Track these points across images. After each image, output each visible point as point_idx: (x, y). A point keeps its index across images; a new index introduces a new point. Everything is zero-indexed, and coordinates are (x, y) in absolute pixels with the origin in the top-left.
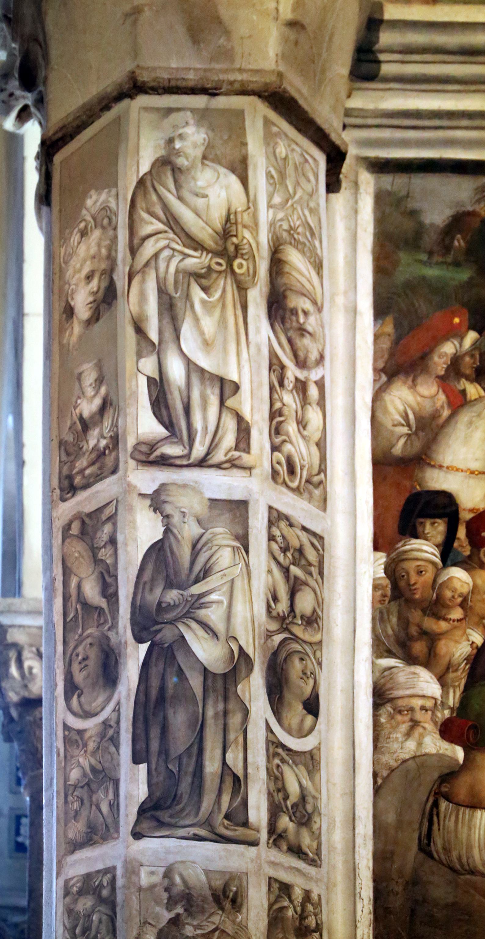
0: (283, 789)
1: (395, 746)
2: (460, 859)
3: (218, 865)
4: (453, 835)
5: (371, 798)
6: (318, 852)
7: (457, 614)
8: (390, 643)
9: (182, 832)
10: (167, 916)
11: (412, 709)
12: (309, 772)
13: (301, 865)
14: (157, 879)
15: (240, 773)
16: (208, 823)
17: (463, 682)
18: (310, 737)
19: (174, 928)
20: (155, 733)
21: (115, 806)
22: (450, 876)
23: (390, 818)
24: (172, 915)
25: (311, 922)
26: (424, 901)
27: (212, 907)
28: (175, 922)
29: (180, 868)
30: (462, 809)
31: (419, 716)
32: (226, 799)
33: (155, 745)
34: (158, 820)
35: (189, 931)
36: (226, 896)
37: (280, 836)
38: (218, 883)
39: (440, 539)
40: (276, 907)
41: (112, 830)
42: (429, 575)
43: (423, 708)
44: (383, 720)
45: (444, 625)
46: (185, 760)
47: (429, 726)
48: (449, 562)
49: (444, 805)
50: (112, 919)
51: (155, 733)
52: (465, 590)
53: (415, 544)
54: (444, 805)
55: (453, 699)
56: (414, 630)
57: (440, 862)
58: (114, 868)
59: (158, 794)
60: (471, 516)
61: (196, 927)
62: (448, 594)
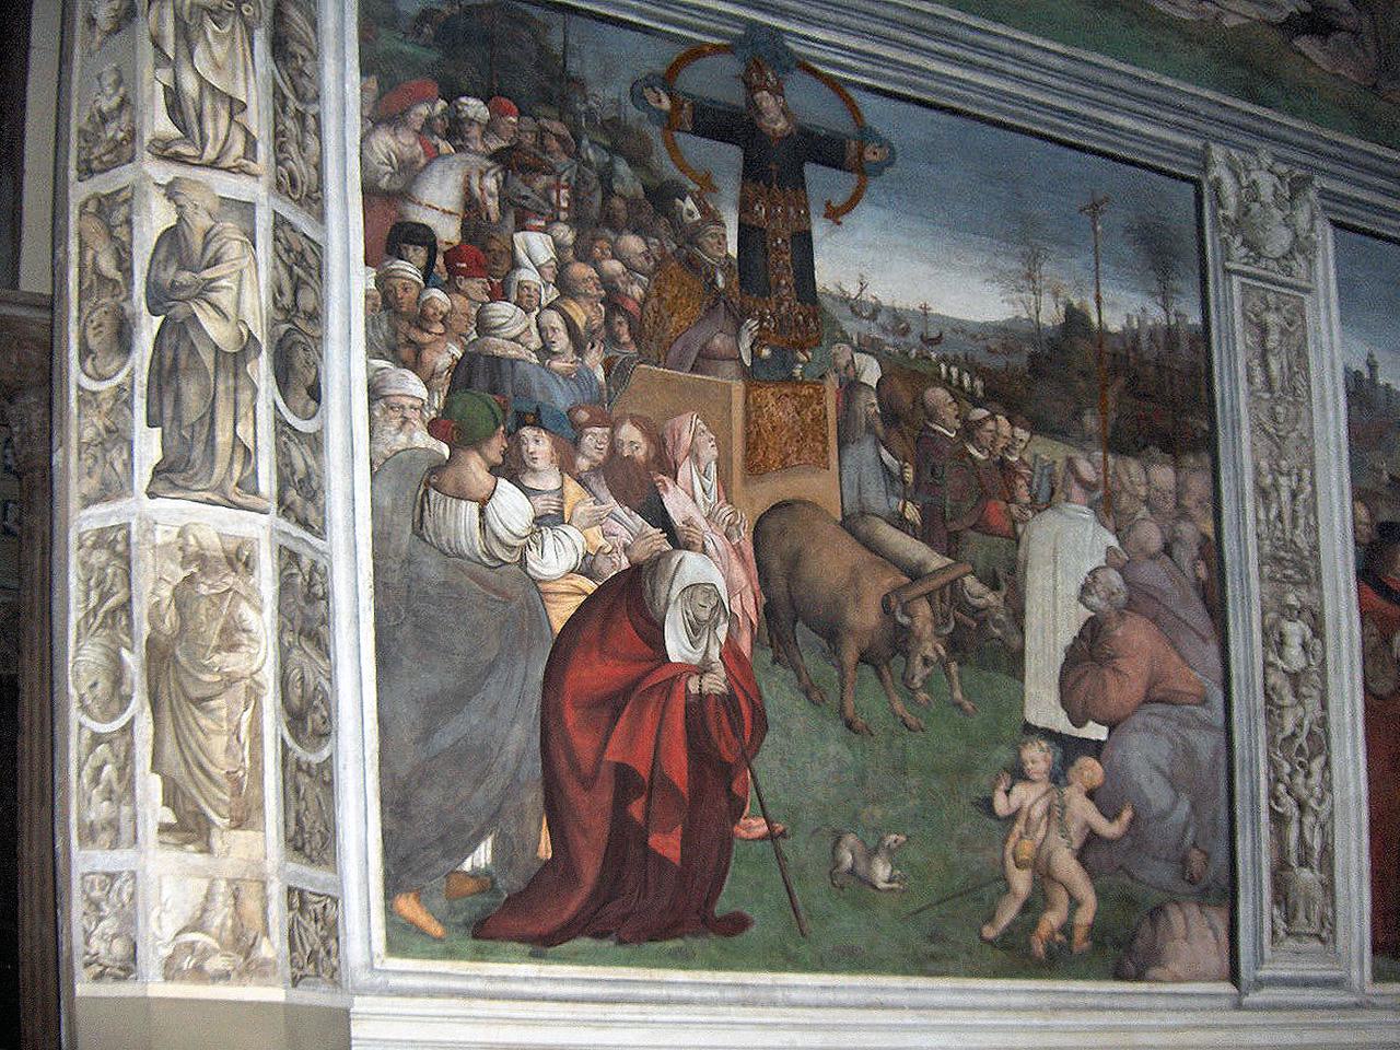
0: (290, 465)
1: (390, 438)
2: (448, 541)
3: (231, 530)
4: (442, 521)
5: (369, 484)
6: (323, 528)
7: (439, 328)
8: (382, 347)
9: (196, 496)
10: (182, 574)
11: (403, 407)
12: (313, 452)
13: (307, 536)
14: (173, 537)
15: (250, 446)
16: (220, 488)
17: (447, 387)
18: (313, 421)
19: (189, 586)
20: (168, 401)
21: (129, 465)
22: (443, 557)
23: (387, 501)
24: (187, 573)
25: (319, 590)
26: (419, 578)
27: (224, 568)
28: (189, 579)
29: (195, 530)
30: (449, 499)
31: (409, 413)
32: (237, 468)
33: (168, 412)
34: (172, 482)
35: (203, 589)
36: (239, 560)
37: (288, 507)
38: (232, 547)
39: (422, 263)
40: (285, 573)
41: (127, 489)
42: (414, 293)
43: (412, 407)
44: (377, 414)
45: (427, 338)
46: (197, 428)
47: (418, 424)
48: (430, 284)
49: (433, 493)
50: (128, 574)
51: (168, 401)
52: (445, 309)
53: (401, 264)
54: (433, 493)
55: (438, 402)
56: (402, 339)
57: (432, 544)
58: (129, 524)
59: (172, 458)
60: (447, 248)
61: (211, 587)
62: (431, 311)
